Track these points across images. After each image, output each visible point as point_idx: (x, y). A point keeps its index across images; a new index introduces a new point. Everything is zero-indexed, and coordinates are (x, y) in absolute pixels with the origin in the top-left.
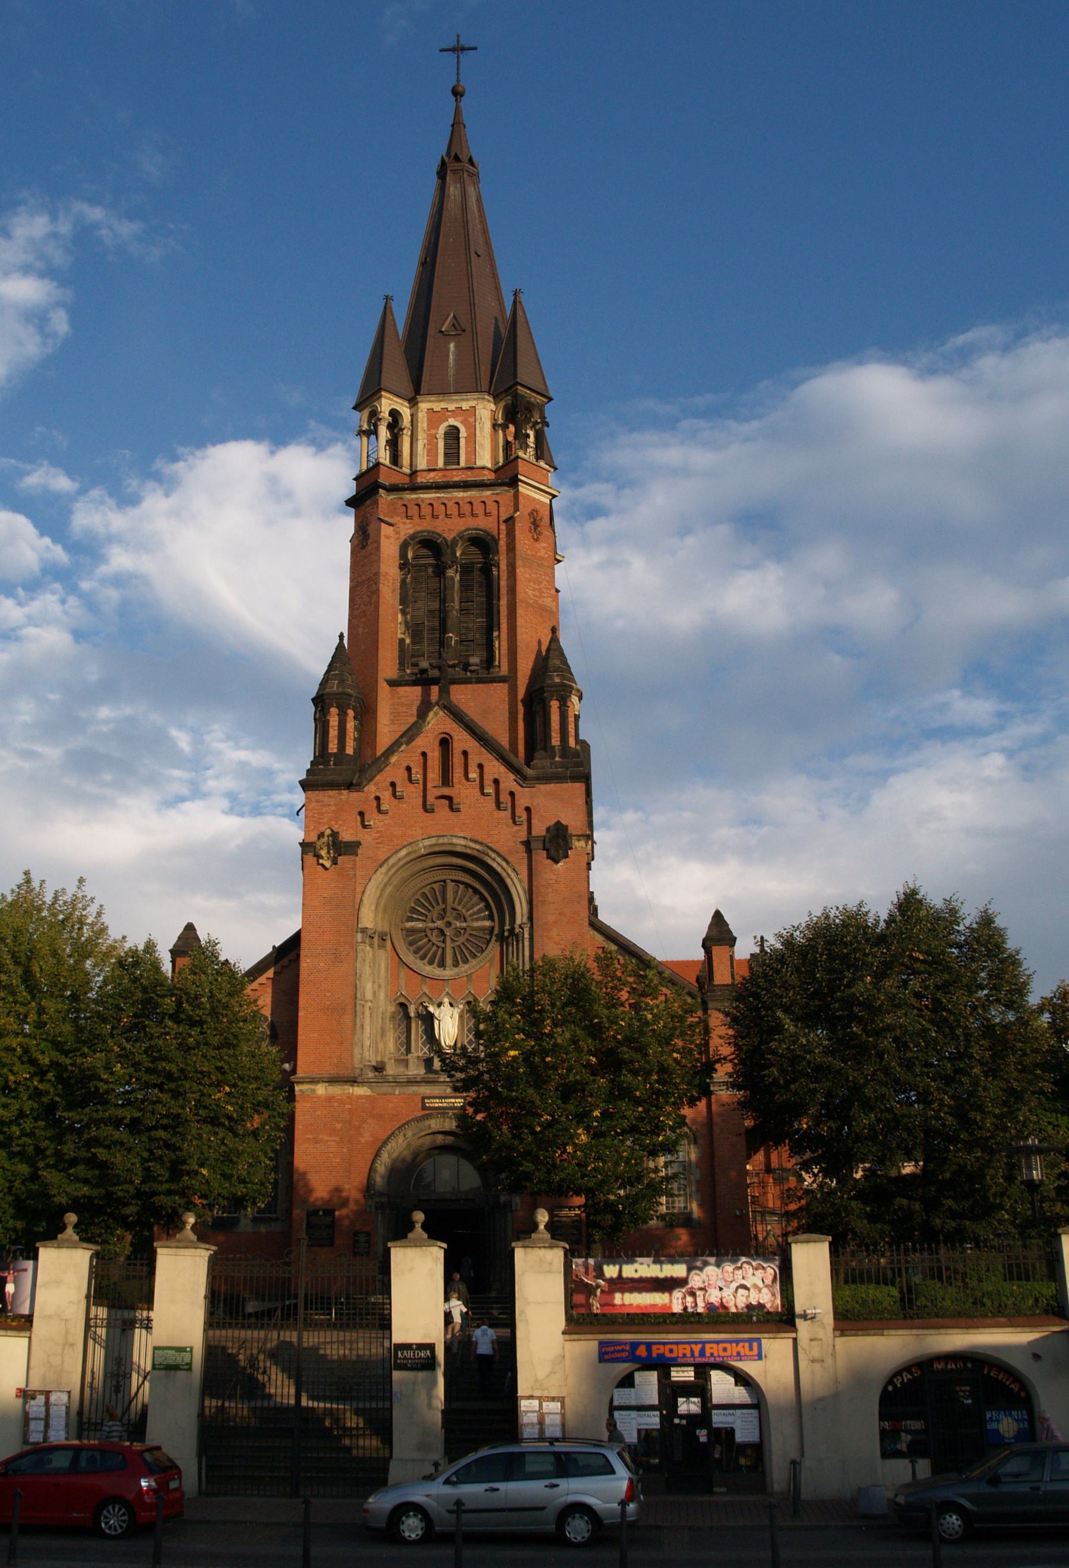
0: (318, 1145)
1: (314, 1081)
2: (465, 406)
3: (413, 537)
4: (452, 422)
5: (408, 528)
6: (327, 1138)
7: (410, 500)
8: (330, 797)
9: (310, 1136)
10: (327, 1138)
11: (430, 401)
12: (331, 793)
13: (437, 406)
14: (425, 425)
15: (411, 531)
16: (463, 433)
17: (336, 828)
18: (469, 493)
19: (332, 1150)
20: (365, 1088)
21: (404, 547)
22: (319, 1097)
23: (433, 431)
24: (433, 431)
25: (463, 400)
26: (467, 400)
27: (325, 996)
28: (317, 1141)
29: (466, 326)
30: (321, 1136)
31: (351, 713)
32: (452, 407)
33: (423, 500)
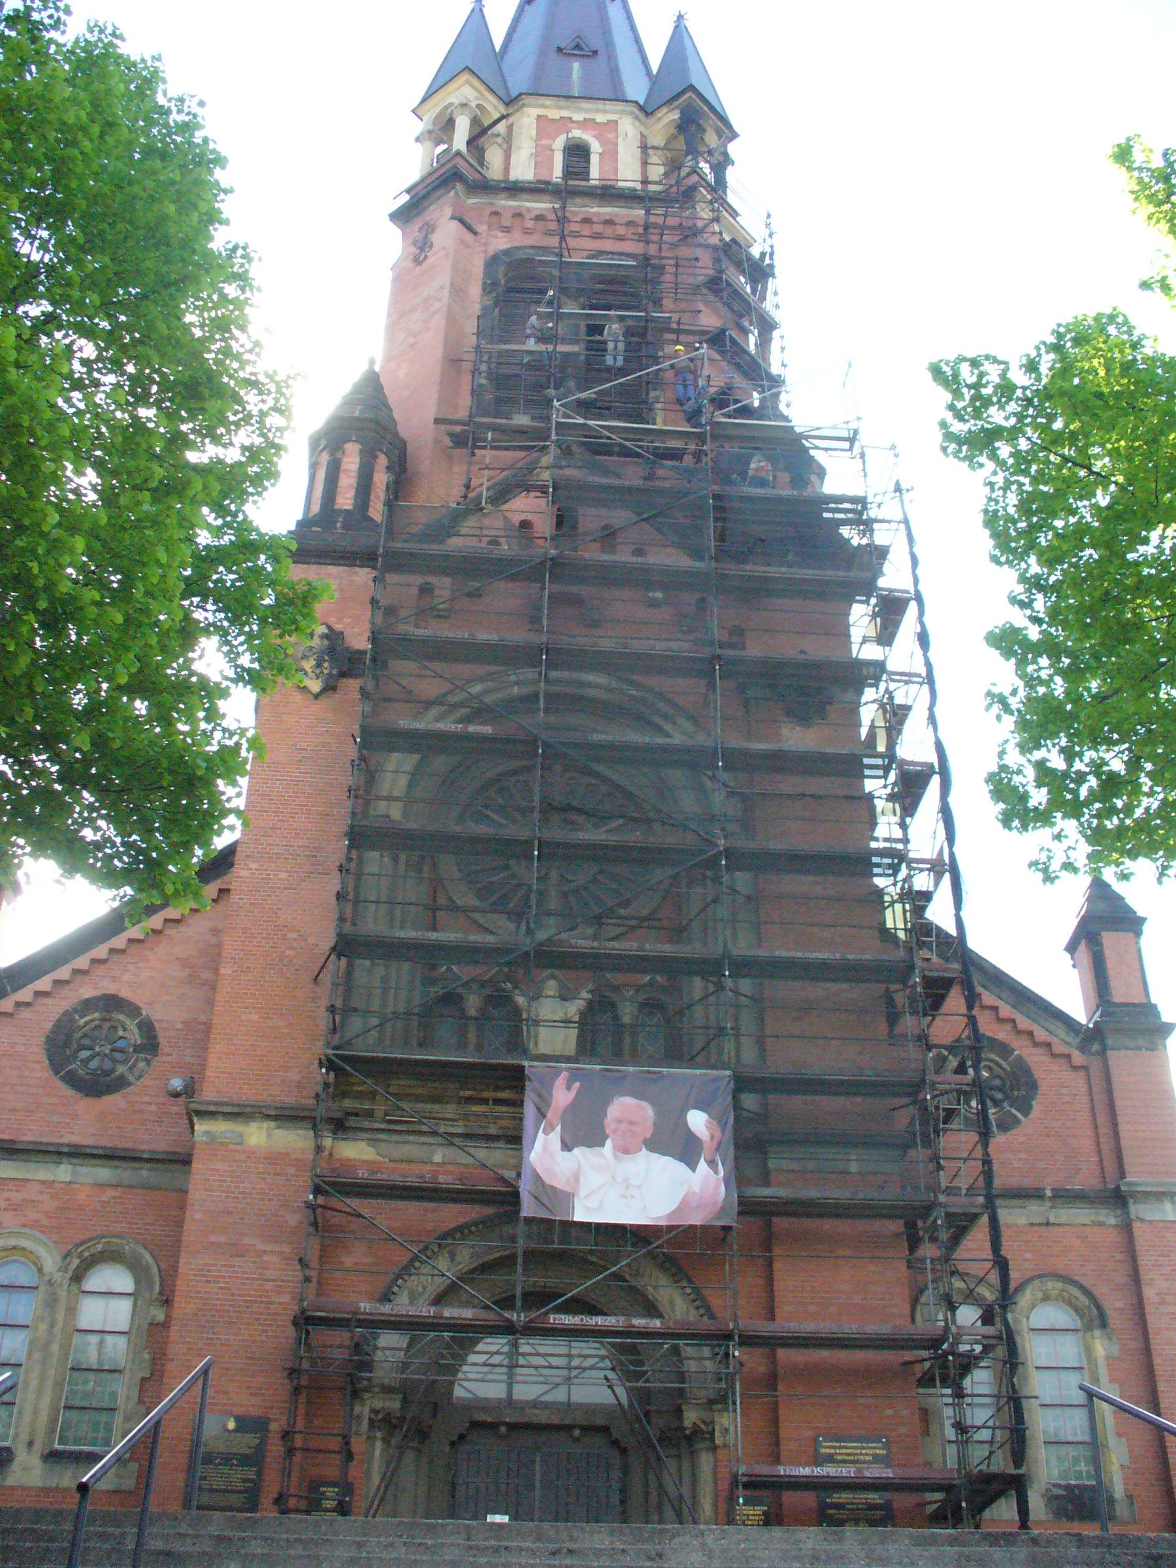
0: (237, 1261)
1: (240, 1113)
2: (600, 118)
3: (507, 252)
4: (576, 133)
5: (501, 243)
6: (261, 1246)
7: (504, 207)
8: (329, 575)
9: (223, 1239)
10: (261, 1246)
11: (543, 106)
12: (333, 570)
13: (554, 114)
14: (534, 132)
15: (505, 247)
16: (596, 147)
17: (338, 627)
18: (608, 210)
19: (270, 1274)
20: (362, 1145)
21: (492, 262)
22: (251, 1154)
23: (545, 142)
24: (545, 142)
25: (598, 111)
26: (605, 112)
27: (285, 938)
28: (239, 1252)
29: (595, 42)
30: (247, 1241)
31: (382, 460)
32: (578, 117)
33: (529, 210)
